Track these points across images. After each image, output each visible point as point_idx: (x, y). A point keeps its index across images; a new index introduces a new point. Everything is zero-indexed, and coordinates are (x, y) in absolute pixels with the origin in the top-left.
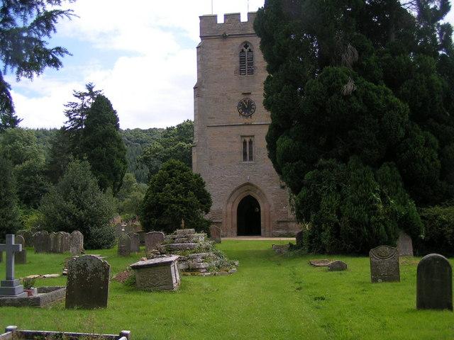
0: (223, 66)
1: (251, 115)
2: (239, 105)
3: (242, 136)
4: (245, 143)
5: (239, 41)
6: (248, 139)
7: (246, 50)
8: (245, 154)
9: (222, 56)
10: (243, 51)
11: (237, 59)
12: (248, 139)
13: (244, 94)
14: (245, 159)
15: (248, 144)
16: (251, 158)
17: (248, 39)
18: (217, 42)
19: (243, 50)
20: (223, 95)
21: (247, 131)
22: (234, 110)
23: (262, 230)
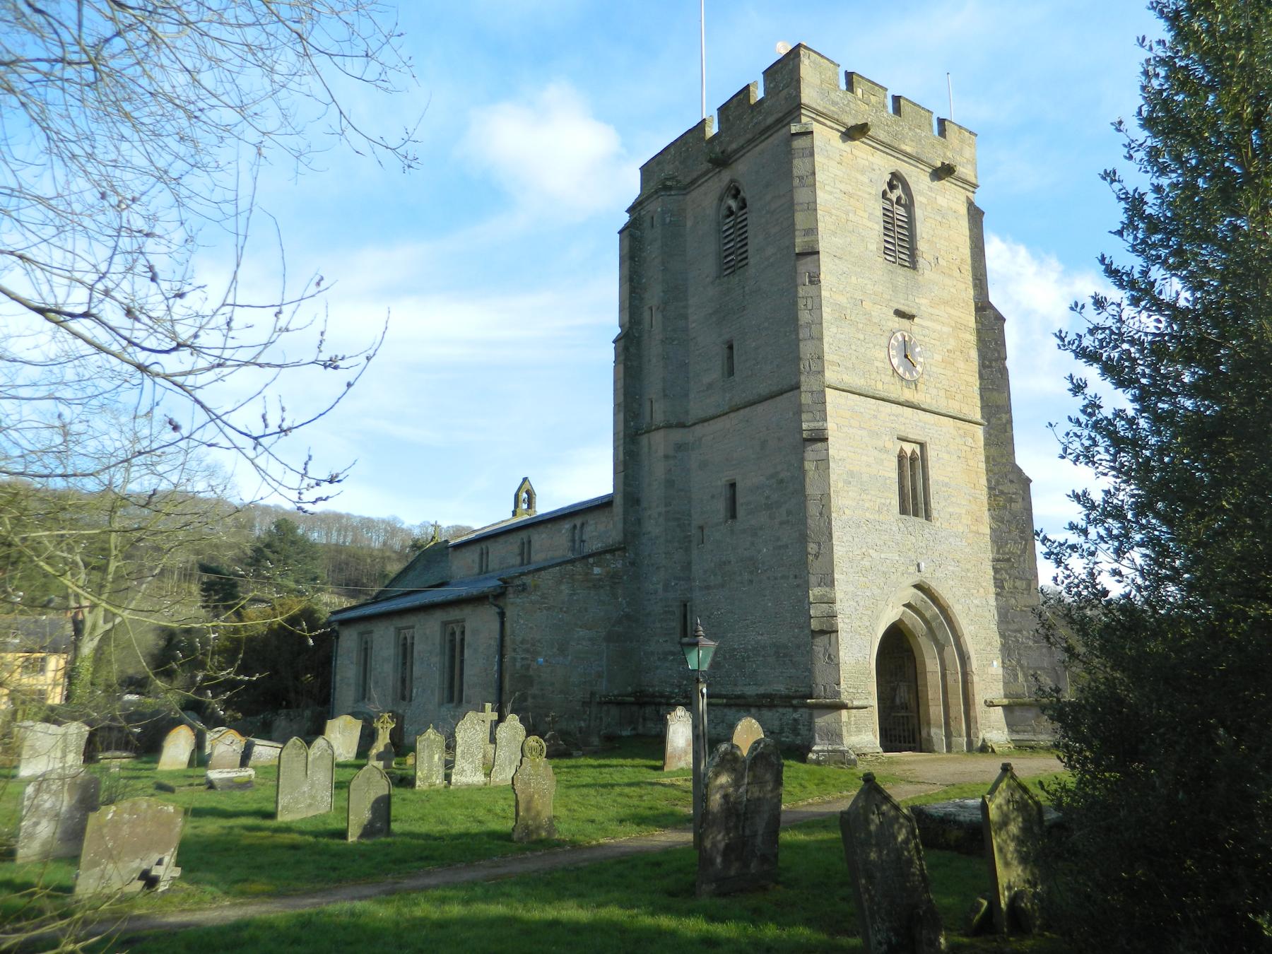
4: (901, 457)
5: (884, 165)
14: (903, 511)
21: (913, 423)
23: (938, 734)
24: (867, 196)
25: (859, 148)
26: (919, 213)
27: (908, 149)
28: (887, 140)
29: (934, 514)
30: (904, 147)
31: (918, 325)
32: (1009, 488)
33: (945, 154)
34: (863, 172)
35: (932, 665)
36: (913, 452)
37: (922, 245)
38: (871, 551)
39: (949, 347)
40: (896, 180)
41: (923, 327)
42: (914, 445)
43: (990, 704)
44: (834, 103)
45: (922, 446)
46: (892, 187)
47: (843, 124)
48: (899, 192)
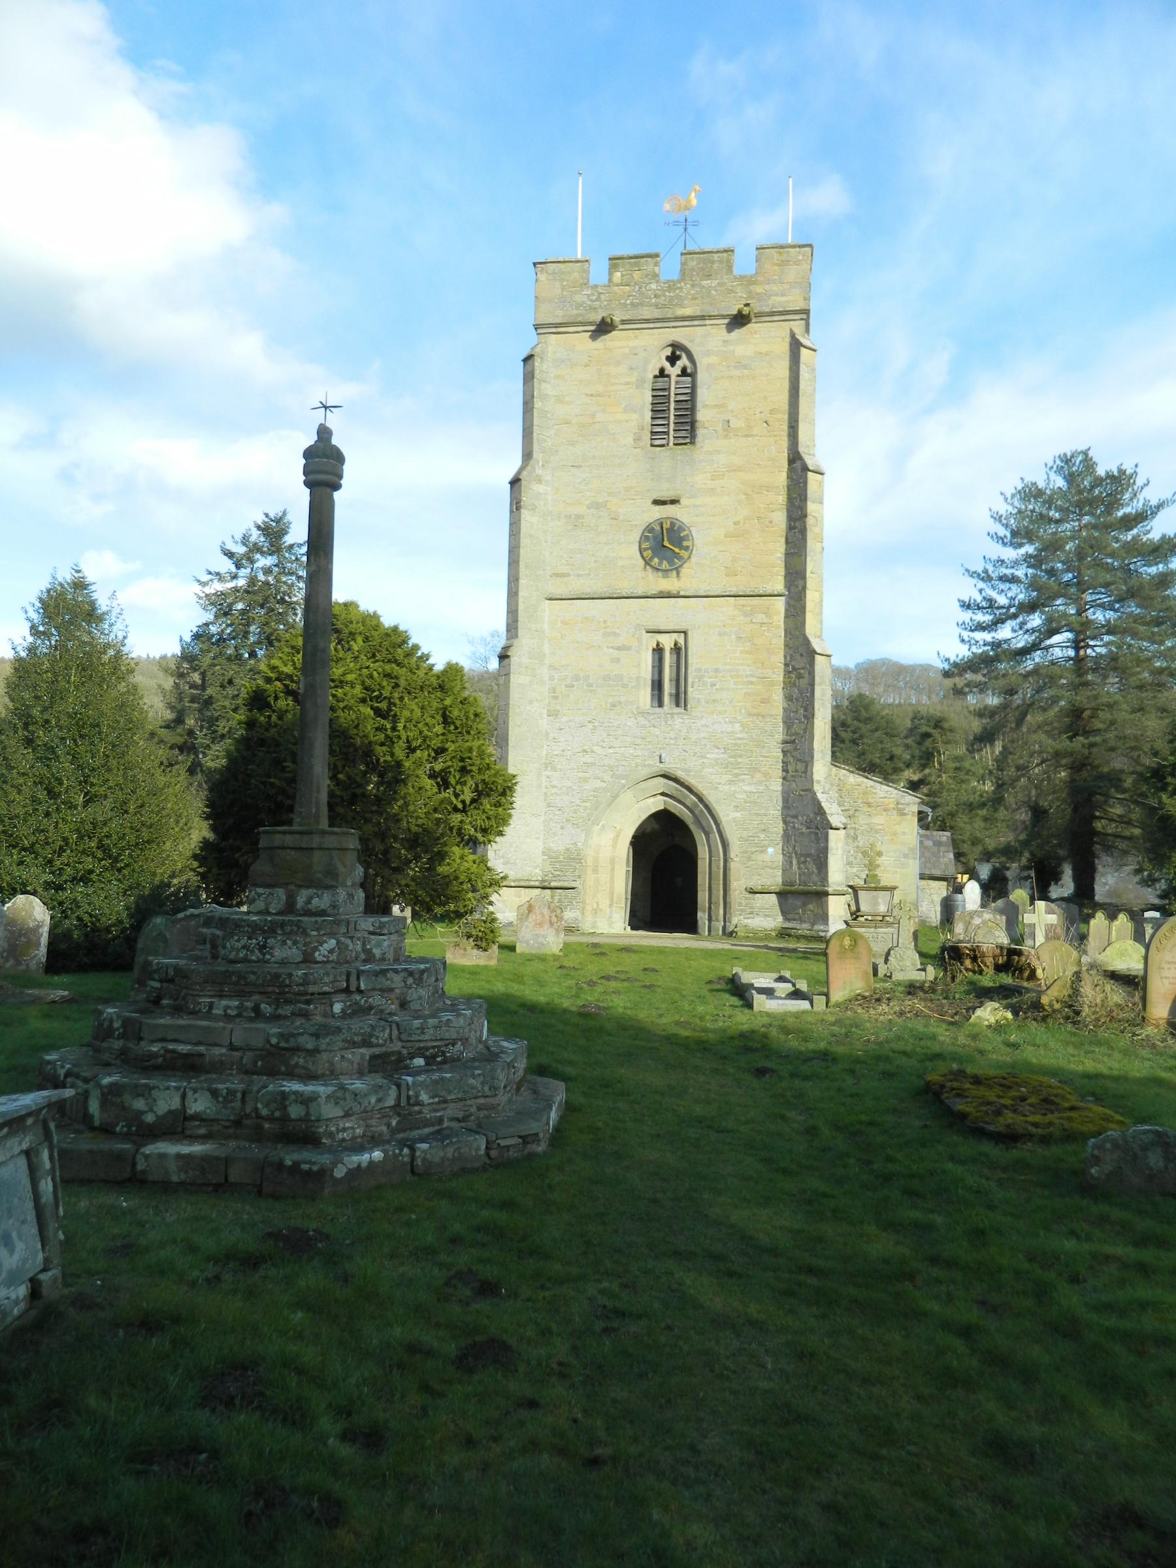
1: (677, 570)
2: (644, 538)
4: (658, 651)
6: (667, 642)
7: (674, 371)
8: (657, 685)
10: (662, 373)
11: (647, 397)
12: (667, 642)
13: (657, 502)
16: (680, 699)
17: (679, 335)
18: (581, 341)
19: (662, 371)
20: (596, 506)
21: (667, 613)
22: (628, 552)
23: (702, 917)
25: (613, 340)
26: (701, 377)
27: (688, 312)
28: (657, 314)
30: (680, 312)
31: (687, 507)
34: (619, 363)
35: (703, 853)
36: (676, 644)
37: (702, 415)
38: (595, 748)
39: (736, 519)
41: (694, 506)
42: (675, 635)
44: (578, 305)
45: (685, 633)
46: (673, 359)
47: (590, 324)
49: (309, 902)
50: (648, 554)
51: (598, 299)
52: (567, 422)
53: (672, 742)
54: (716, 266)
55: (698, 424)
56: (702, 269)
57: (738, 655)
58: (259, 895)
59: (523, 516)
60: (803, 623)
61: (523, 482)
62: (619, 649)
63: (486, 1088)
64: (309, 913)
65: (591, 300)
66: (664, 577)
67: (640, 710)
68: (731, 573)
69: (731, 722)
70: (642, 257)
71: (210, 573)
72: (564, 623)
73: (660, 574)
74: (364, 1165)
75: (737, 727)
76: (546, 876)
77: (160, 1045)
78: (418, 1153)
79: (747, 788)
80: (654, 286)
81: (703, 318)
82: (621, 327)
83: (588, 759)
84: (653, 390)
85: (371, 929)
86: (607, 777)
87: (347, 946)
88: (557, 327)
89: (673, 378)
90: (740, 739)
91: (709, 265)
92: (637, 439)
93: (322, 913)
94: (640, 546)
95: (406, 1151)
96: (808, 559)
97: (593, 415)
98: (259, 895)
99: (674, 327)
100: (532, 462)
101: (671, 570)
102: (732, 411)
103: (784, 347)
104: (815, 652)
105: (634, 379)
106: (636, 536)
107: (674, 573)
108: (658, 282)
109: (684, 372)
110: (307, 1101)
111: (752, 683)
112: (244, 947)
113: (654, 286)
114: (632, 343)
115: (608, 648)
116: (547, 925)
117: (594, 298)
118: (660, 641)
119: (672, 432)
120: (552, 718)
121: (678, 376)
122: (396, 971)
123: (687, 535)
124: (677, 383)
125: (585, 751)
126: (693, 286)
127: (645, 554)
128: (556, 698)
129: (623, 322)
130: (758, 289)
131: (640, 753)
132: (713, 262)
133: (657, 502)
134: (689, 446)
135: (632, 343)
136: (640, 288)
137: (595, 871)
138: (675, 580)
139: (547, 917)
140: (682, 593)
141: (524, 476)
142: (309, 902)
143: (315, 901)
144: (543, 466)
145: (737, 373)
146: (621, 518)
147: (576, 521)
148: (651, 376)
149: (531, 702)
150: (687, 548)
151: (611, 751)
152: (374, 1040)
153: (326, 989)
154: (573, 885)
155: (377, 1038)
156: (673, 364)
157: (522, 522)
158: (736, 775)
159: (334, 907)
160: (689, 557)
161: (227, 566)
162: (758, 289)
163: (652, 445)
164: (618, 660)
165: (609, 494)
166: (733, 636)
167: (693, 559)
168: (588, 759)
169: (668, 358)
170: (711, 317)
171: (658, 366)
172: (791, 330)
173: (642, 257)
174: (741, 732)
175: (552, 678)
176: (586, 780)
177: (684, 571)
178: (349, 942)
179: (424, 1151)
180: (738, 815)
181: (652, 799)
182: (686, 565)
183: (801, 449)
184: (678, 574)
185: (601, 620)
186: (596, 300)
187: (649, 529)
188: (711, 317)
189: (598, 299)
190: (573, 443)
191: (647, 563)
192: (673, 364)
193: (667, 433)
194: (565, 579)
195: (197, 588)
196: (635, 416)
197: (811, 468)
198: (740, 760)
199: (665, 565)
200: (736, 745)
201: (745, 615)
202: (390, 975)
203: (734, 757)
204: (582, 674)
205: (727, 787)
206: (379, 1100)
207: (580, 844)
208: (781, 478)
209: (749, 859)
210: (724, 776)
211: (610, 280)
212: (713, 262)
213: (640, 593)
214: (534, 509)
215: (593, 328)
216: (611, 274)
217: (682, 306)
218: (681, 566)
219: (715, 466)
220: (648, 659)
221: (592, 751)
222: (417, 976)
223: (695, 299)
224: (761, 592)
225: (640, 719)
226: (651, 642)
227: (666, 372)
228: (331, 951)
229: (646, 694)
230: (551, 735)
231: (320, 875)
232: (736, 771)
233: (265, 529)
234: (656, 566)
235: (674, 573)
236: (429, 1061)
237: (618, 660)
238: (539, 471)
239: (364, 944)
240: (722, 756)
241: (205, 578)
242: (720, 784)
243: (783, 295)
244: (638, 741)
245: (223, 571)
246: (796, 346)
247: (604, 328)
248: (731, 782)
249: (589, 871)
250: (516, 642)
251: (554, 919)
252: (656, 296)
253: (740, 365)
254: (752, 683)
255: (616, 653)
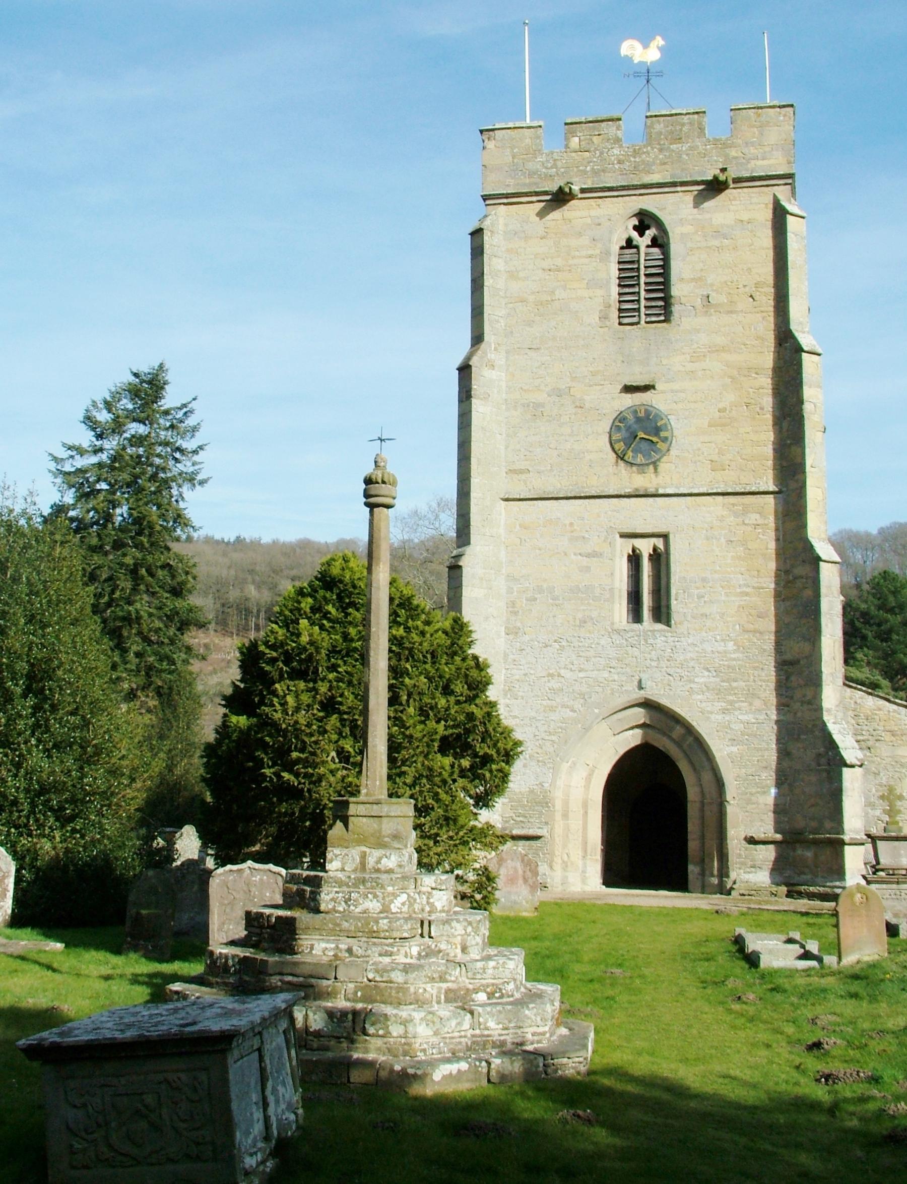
0: (560, 294)
1: (655, 464)
3: (623, 536)
4: (634, 559)
6: (645, 547)
7: (643, 242)
8: (635, 598)
9: (559, 262)
13: (629, 389)
14: (636, 616)
15: (646, 567)
16: (662, 613)
17: (650, 203)
20: (558, 393)
23: (693, 869)
24: (587, 261)
25: (574, 210)
26: (675, 248)
27: (656, 178)
29: (675, 617)
31: (663, 392)
32: (800, 570)
33: (726, 156)
34: (580, 234)
35: (692, 793)
36: (655, 549)
37: (676, 290)
38: (562, 672)
39: (721, 406)
40: (645, 221)
41: (672, 391)
42: (654, 541)
43: (751, 841)
44: (531, 174)
45: (665, 537)
46: (641, 229)
47: (545, 193)
48: (650, 233)
49: (379, 861)
50: (620, 446)
51: (555, 166)
52: (523, 301)
53: (654, 664)
54: (685, 129)
55: (673, 301)
56: (672, 132)
57: (729, 561)
58: (336, 856)
59: (474, 406)
60: (803, 526)
61: (473, 369)
62: (588, 556)
63: (539, 1019)
64: (378, 871)
65: (546, 168)
66: (639, 473)
67: (615, 627)
68: (716, 466)
69: (723, 640)
70: (602, 121)
71: (70, 448)
72: (524, 527)
73: (634, 468)
74: (454, 1072)
75: (731, 646)
76: (507, 822)
77: (278, 977)
78: (493, 1066)
79: (744, 718)
80: (616, 151)
81: (674, 184)
82: (580, 196)
83: (554, 684)
84: (619, 263)
85: (434, 885)
86: (577, 705)
87: (415, 900)
88: (509, 198)
89: (643, 250)
90: (734, 659)
91: (678, 128)
92: (604, 317)
93: (390, 871)
94: (610, 437)
95: (484, 1064)
96: (807, 451)
97: (553, 292)
98: (336, 856)
99: (641, 195)
100: (483, 346)
101: (648, 465)
102: (712, 285)
103: (766, 215)
104: (818, 559)
105: (598, 252)
106: (606, 425)
107: (651, 467)
108: (621, 146)
109: (655, 243)
110: (405, 1023)
111: (747, 594)
112: (332, 900)
113: (616, 151)
114: (593, 213)
115: (575, 554)
116: (521, 881)
117: (549, 165)
118: (637, 546)
119: (643, 310)
120: (511, 637)
121: (648, 246)
122: (458, 921)
123: (665, 425)
124: (647, 254)
125: (551, 675)
126: (661, 150)
127: (617, 447)
128: (516, 613)
129: (583, 191)
130: (733, 153)
131: (616, 677)
132: (683, 125)
133: (629, 389)
134: (664, 324)
135: (593, 213)
136: (602, 153)
137: (565, 816)
138: (653, 476)
139: (520, 872)
140: (661, 491)
141: (474, 362)
142: (379, 861)
143: (384, 860)
144: (496, 349)
145: (716, 243)
146: (587, 405)
147: (536, 411)
148: (616, 249)
149: (487, 618)
150: (665, 440)
151: (582, 675)
152: (447, 977)
153: (405, 935)
154: (539, 833)
155: (450, 975)
156: (641, 235)
157: (473, 413)
158: (731, 703)
159: (400, 866)
160: (669, 450)
161: (86, 438)
162: (733, 153)
163: (620, 324)
164: (587, 569)
165: (574, 379)
166: (723, 540)
167: (673, 452)
168: (554, 684)
169: (635, 228)
170: (683, 184)
171: (626, 236)
172: (774, 195)
173: (602, 121)
174: (735, 651)
175: (510, 590)
176: (552, 709)
177: (662, 466)
178: (417, 896)
179: (498, 1066)
180: (734, 749)
181: (631, 732)
182: (664, 459)
183: (793, 327)
184: (656, 469)
185: (567, 522)
186: (552, 168)
187: (620, 418)
188: (683, 184)
189: (555, 166)
190: (530, 323)
191: (621, 457)
192: (641, 235)
193: (638, 310)
194: (523, 477)
195: (53, 466)
196: (599, 292)
197: (805, 349)
198: (734, 684)
199: (640, 459)
200: (729, 667)
201: (736, 515)
202: (454, 924)
203: (728, 681)
204: (545, 586)
205: (720, 717)
206: (458, 1024)
207: (546, 785)
208: (768, 359)
209: (749, 802)
210: (716, 704)
211: (567, 146)
212: (683, 125)
213: (612, 493)
214: (486, 397)
215: (548, 197)
216: (567, 139)
217: (649, 172)
218: (659, 460)
219: (695, 346)
220: (623, 568)
221: (559, 675)
222: (475, 925)
223: (665, 164)
224: (753, 489)
225: (615, 636)
226: (626, 547)
227: (634, 243)
228: (403, 904)
229: (621, 607)
230: (511, 656)
231: (386, 839)
232: (731, 698)
233: (134, 392)
234: (630, 460)
235: (651, 467)
236: (490, 995)
237: (587, 569)
238: (491, 356)
239: (428, 898)
240: (712, 679)
241: (63, 453)
242: (712, 713)
243: (763, 159)
244: (614, 663)
245: (85, 445)
246: (780, 215)
247: (561, 198)
248: (724, 711)
249: (558, 816)
250: (468, 550)
251: (529, 874)
252: (619, 162)
253: (718, 233)
254: (747, 594)
255: (585, 561)
